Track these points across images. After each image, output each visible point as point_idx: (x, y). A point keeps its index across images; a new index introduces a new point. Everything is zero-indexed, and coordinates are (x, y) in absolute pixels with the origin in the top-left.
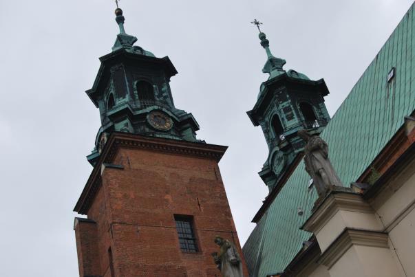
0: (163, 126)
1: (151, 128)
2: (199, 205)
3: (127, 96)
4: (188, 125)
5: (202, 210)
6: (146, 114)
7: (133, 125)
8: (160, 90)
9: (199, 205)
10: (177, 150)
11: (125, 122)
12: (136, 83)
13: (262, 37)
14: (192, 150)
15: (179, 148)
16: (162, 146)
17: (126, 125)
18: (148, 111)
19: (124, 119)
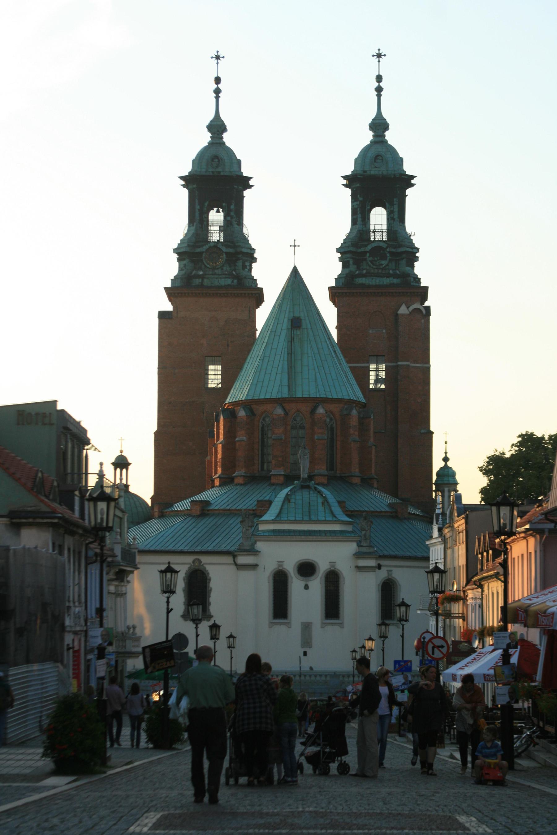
0: (216, 263)
1: (205, 266)
2: (228, 345)
3: (195, 224)
4: (240, 256)
5: (230, 351)
6: (203, 252)
7: (192, 261)
8: (229, 207)
9: (228, 345)
10: (219, 295)
11: (184, 262)
12: (206, 204)
13: (379, 78)
14: (231, 293)
15: (220, 294)
16: (206, 294)
17: (185, 266)
18: (204, 251)
19: (184, 259)
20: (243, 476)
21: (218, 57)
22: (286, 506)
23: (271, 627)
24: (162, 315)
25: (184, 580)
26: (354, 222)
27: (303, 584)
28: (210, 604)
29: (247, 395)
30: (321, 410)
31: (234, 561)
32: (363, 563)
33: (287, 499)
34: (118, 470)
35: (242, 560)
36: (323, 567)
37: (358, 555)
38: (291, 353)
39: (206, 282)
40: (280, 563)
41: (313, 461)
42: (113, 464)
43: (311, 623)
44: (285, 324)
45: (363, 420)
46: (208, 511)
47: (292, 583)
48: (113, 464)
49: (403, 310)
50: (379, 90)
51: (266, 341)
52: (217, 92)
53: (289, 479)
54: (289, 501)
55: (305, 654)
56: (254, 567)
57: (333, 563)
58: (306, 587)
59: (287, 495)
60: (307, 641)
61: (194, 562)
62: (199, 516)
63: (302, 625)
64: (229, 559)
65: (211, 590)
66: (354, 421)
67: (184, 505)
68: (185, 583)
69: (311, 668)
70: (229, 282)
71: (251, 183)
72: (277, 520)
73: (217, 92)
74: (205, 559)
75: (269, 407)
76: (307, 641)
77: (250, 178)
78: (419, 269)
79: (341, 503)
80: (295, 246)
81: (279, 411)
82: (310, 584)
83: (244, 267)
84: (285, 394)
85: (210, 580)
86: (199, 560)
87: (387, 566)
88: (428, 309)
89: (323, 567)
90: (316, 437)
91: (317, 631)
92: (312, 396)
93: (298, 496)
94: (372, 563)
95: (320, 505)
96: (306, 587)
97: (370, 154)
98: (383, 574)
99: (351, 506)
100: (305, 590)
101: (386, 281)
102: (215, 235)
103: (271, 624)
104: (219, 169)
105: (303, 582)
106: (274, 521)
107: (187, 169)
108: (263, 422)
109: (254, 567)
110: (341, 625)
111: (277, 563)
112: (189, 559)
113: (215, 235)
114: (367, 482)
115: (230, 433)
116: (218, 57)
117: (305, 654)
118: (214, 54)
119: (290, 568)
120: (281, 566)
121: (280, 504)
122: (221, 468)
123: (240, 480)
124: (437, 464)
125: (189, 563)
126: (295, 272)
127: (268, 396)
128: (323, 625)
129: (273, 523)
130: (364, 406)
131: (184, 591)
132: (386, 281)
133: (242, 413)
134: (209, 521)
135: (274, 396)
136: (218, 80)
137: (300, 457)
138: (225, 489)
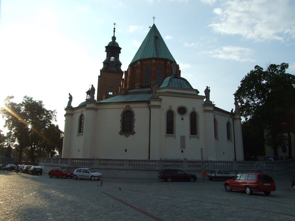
20: (139, 85)
21: (115, 24)
22: (170, 83)
23: (166, 138)
24: (99, 76)
25: (121, 116)
27: (181, 117)
28: (134, 127)
29: (140, 57)
31: (148, 106)
33: (171, 80)
34: (88, 95)
35: (153, 103)
36: (189, 110)
38: (156, 45)
39: (110, 69)
40: (170, 107)
42: (86, 92)
43: (185, 136)
44: (153, 38)
46: (128, 93)
47: (176, 116)
48: (86, 92)
51: (146, 43)
52: (114, 31)
54: (171, 81)
55: (182, 151)
56: (159, 107)
57: (194, 108)
58: (182, 119)
59: (171, 78)
60: (183, 146)
61: (126, 107)
62: (124, 95)
63: (180, 137)
64: (145, 105)
65: (135, 120)
68: (121, 117)
69: (185, 159)
70: (116, 70)
71: (121, 51)
72: (168, 87)
73: (114, 31)
74: (132, 106)
76: (183, 146)
77: (121, 49)
80: (154, 18)
81: (154, 61)
82: (184, 117)
83: (119, 67)
84: (156, 57)
85: (134, 115)
86: (129, 106)
87: (215, 113)
89: (189, 110)
90: (167, 72)
92: (165, 58)
93: (175, 79)
95: (185, 83)
96: (182, 119)
100: (181, 120)
103: (166, 136)
104: (115, 46)
105: (181, 116)
106: (168, 87)
107: (107, 45)
108: (146, 68)
109: (159, 107)
110: (198, 138)
111: (169, 107)
112: (124, 106)
116: (115, 24)
117: (182, 151)
118: (114, 23)
119: (175, 109)
120: (171, 108)
121: (168, 82)
122: (128, 85)
123: (138, 87)
125: (123, 108)
127: (149, 57)
128: (190, 138)
129: (166, 88)
131: (120, 121)
135: (151, 57)
136: (114, 29)
137: (173, 66)
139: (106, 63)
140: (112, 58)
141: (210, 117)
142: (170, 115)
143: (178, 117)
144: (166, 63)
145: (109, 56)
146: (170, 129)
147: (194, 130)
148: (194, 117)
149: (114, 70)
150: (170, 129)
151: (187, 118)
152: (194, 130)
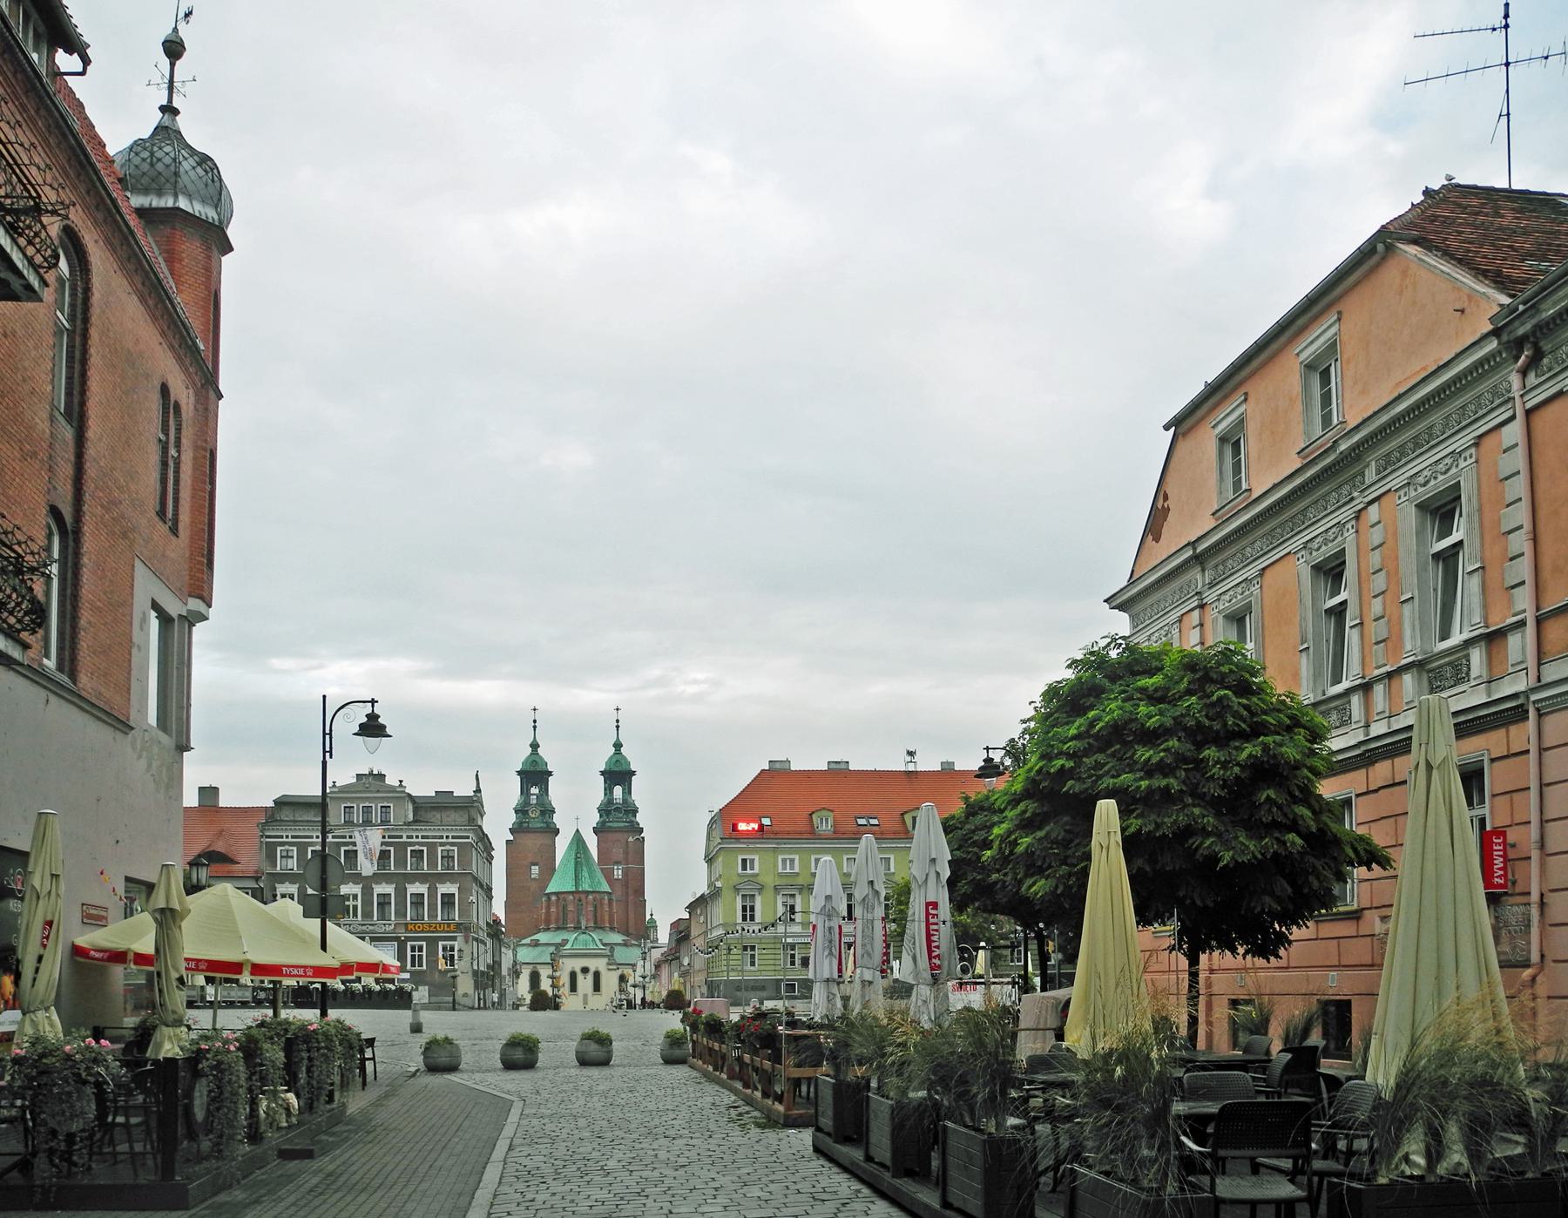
26: (605, 795)
30: (590, 897)
32: (610, 967)
33: (576, 938)
36: (592, 970)
37: (608, 964)
41: (587, 921)
45: (610, 900)
49: (631, 839)
50: (618, 727)
52: (535, 727)
53: (577, 928)
60: (585, 1002)
66: (606, 902)
67: (527, 941)
73: (535, 727)
74: (538, 966)
75: (566, 895)
76: (585, 1002)
78: (639, 818)
79: (600, 940)
81: (571, 897)
84: (574, 889)
88: (643, 838)
89: (592, 970)
91: (590, 998)
94: (615, 967)
97: (614, 760)
98: (619, 972)
99: (604, 941)
101: (622, 825)
102: (533, 800)
112: (531, 966)
113: (533, 800)
114: (612, 929)
115: (548, 907)
119: (578, 970)
124: (648, 917)
126: (578, 830)
130: (610, 893)
132: (622, 825)
133: (554, 898)
134: (540, 948)
136: (535, 721)
138: (546, 933)
139: (521, 811)
140: (534, 790)
141: (615, 976)
142: (573, 976)
143: (580, 977)
144: (587, 897)
145: (525, 791)
146: (573, 988)
147: (597, 987)
148: (597, 975)
149: (539, 825)
150: (573, 988)
151: (590, 977)
152: (597, 987)
